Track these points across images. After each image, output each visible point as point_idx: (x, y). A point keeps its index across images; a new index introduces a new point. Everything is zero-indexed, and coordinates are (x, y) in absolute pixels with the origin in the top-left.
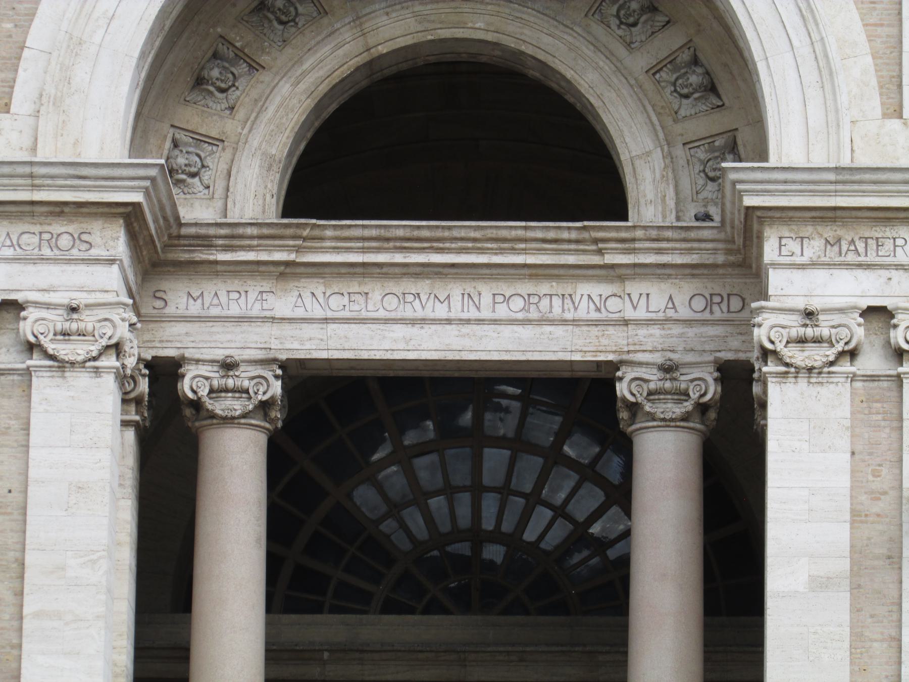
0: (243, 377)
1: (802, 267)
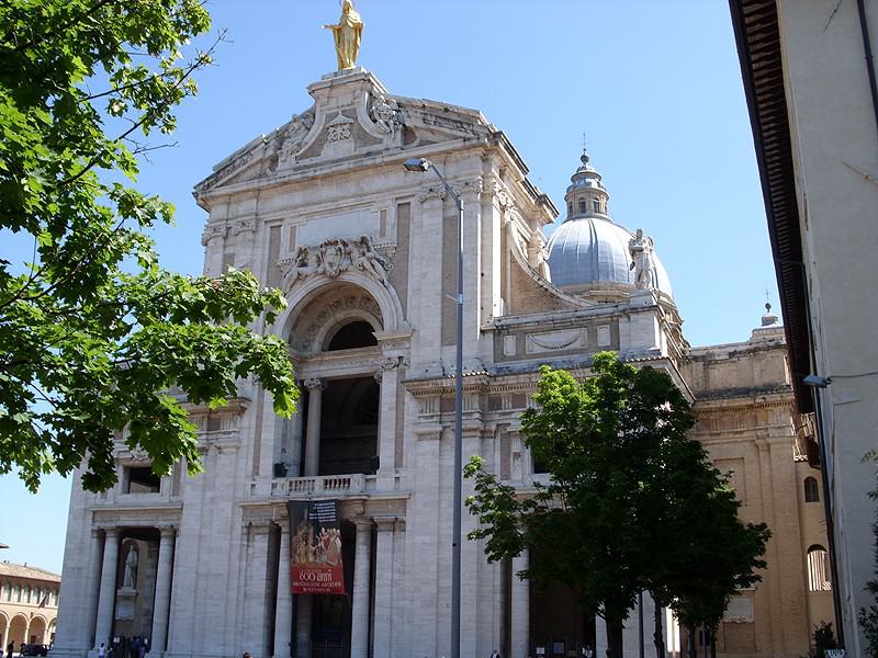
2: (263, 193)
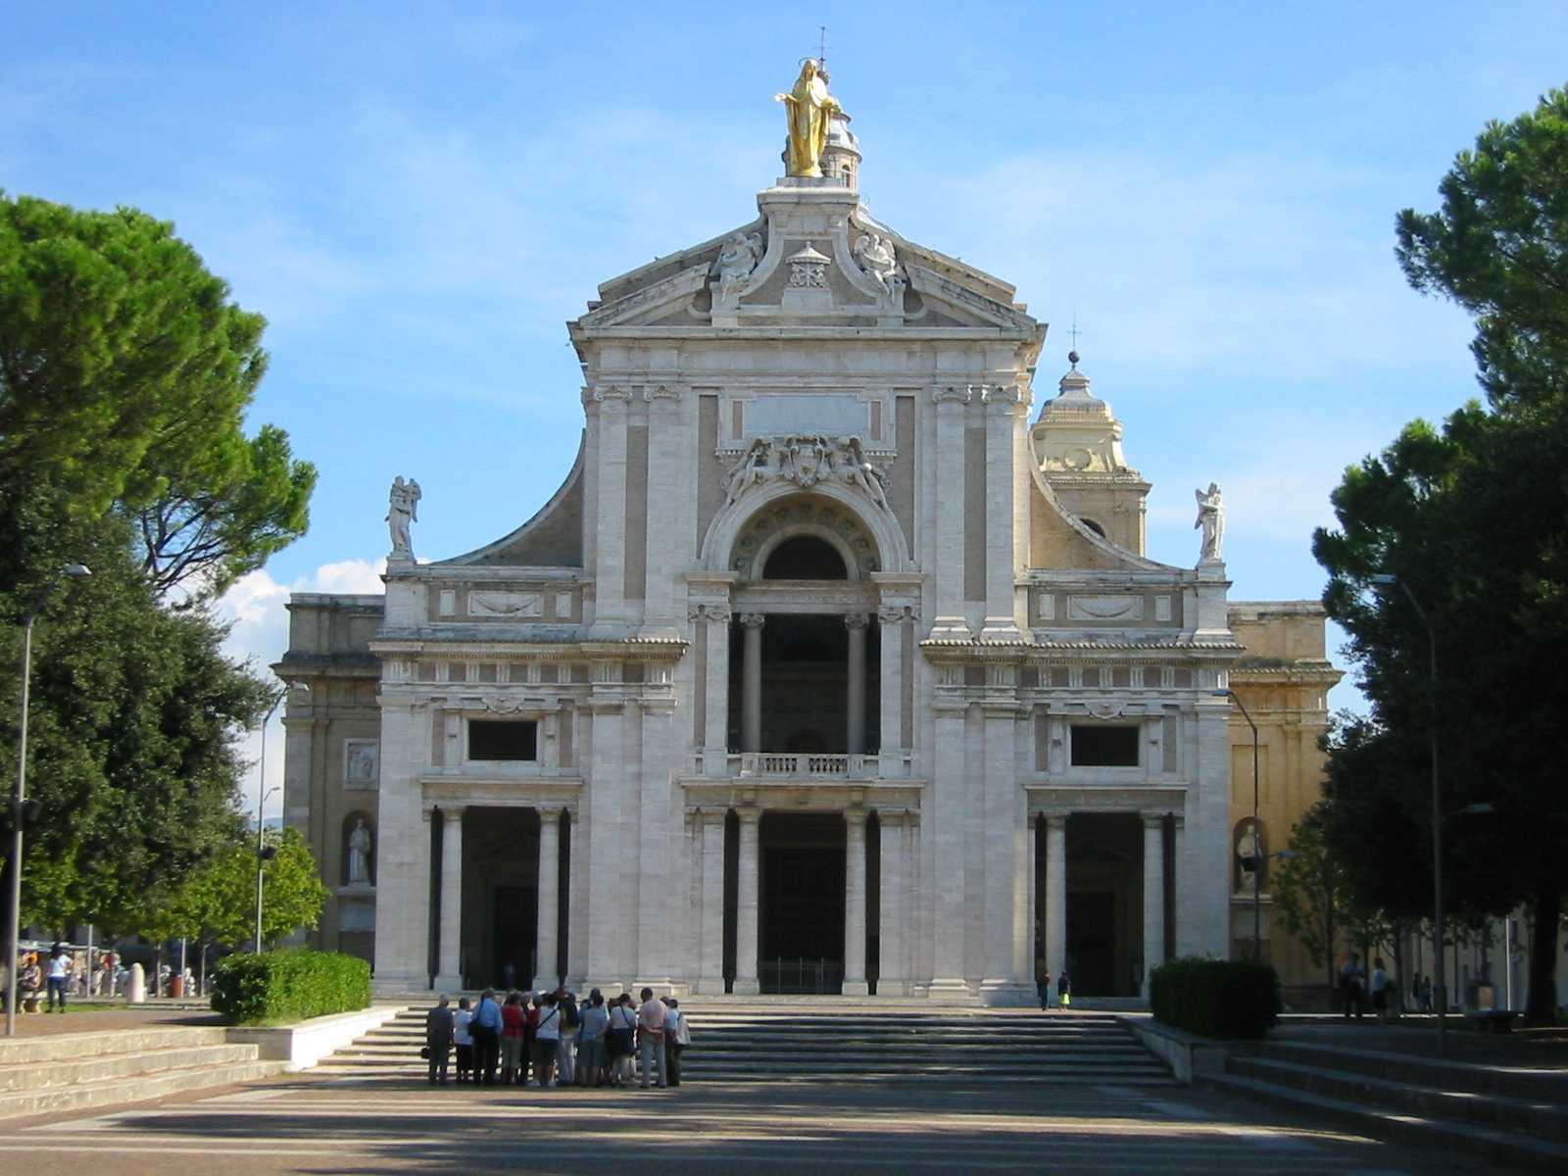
0: (755, 617)
2: (689, 345)
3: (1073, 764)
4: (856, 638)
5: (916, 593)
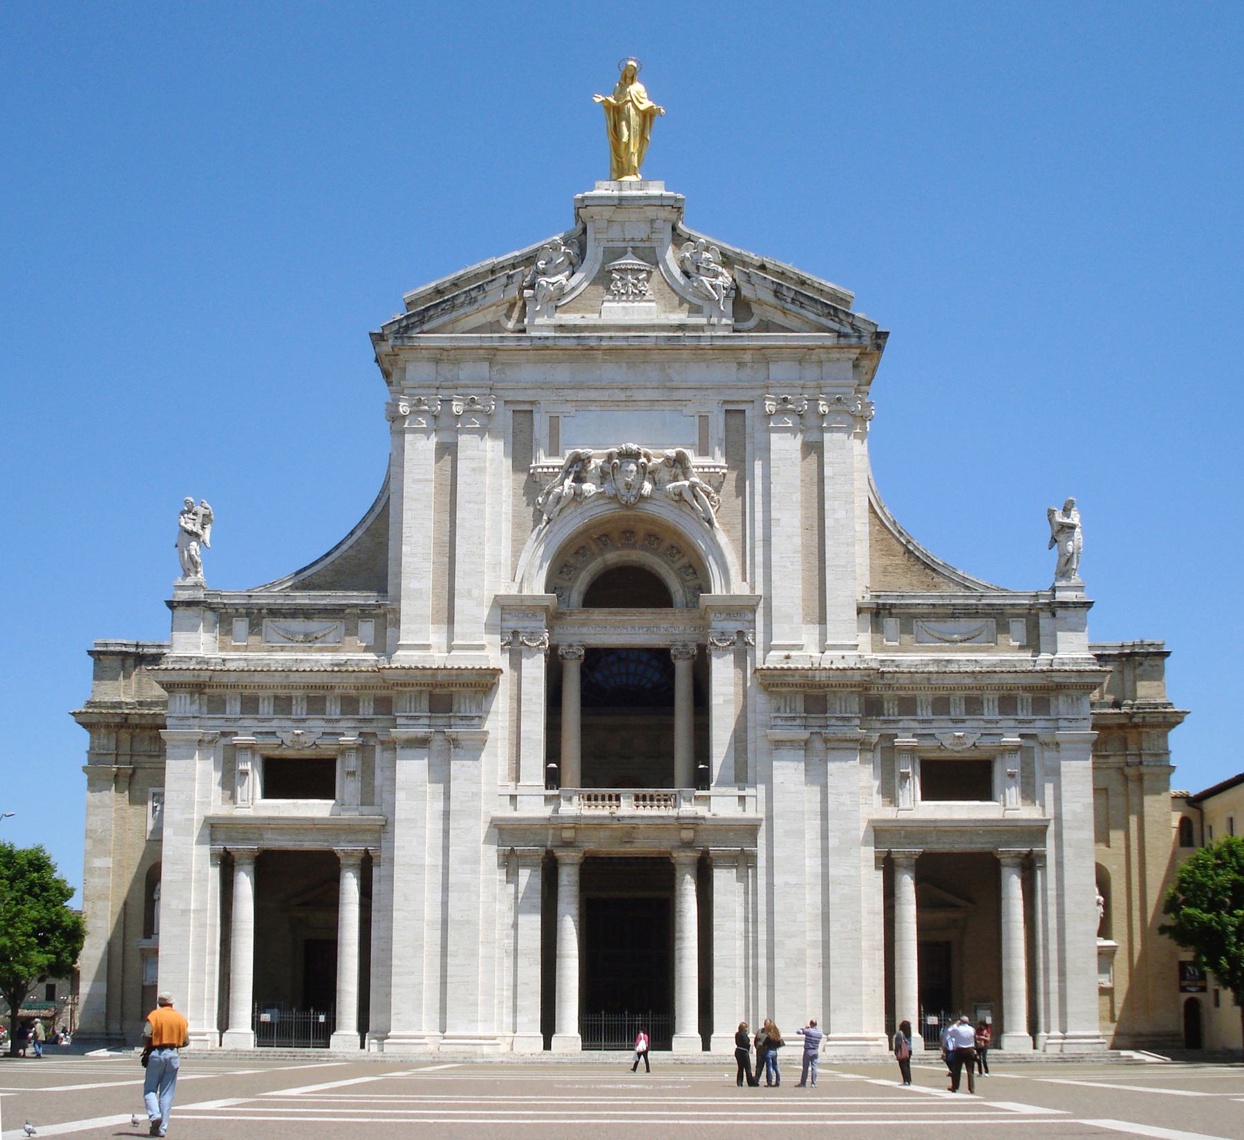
1: (720, 621)
2: (501, 357)
3: (923, 799)
4: (682, 670)
5: (750, 617)
